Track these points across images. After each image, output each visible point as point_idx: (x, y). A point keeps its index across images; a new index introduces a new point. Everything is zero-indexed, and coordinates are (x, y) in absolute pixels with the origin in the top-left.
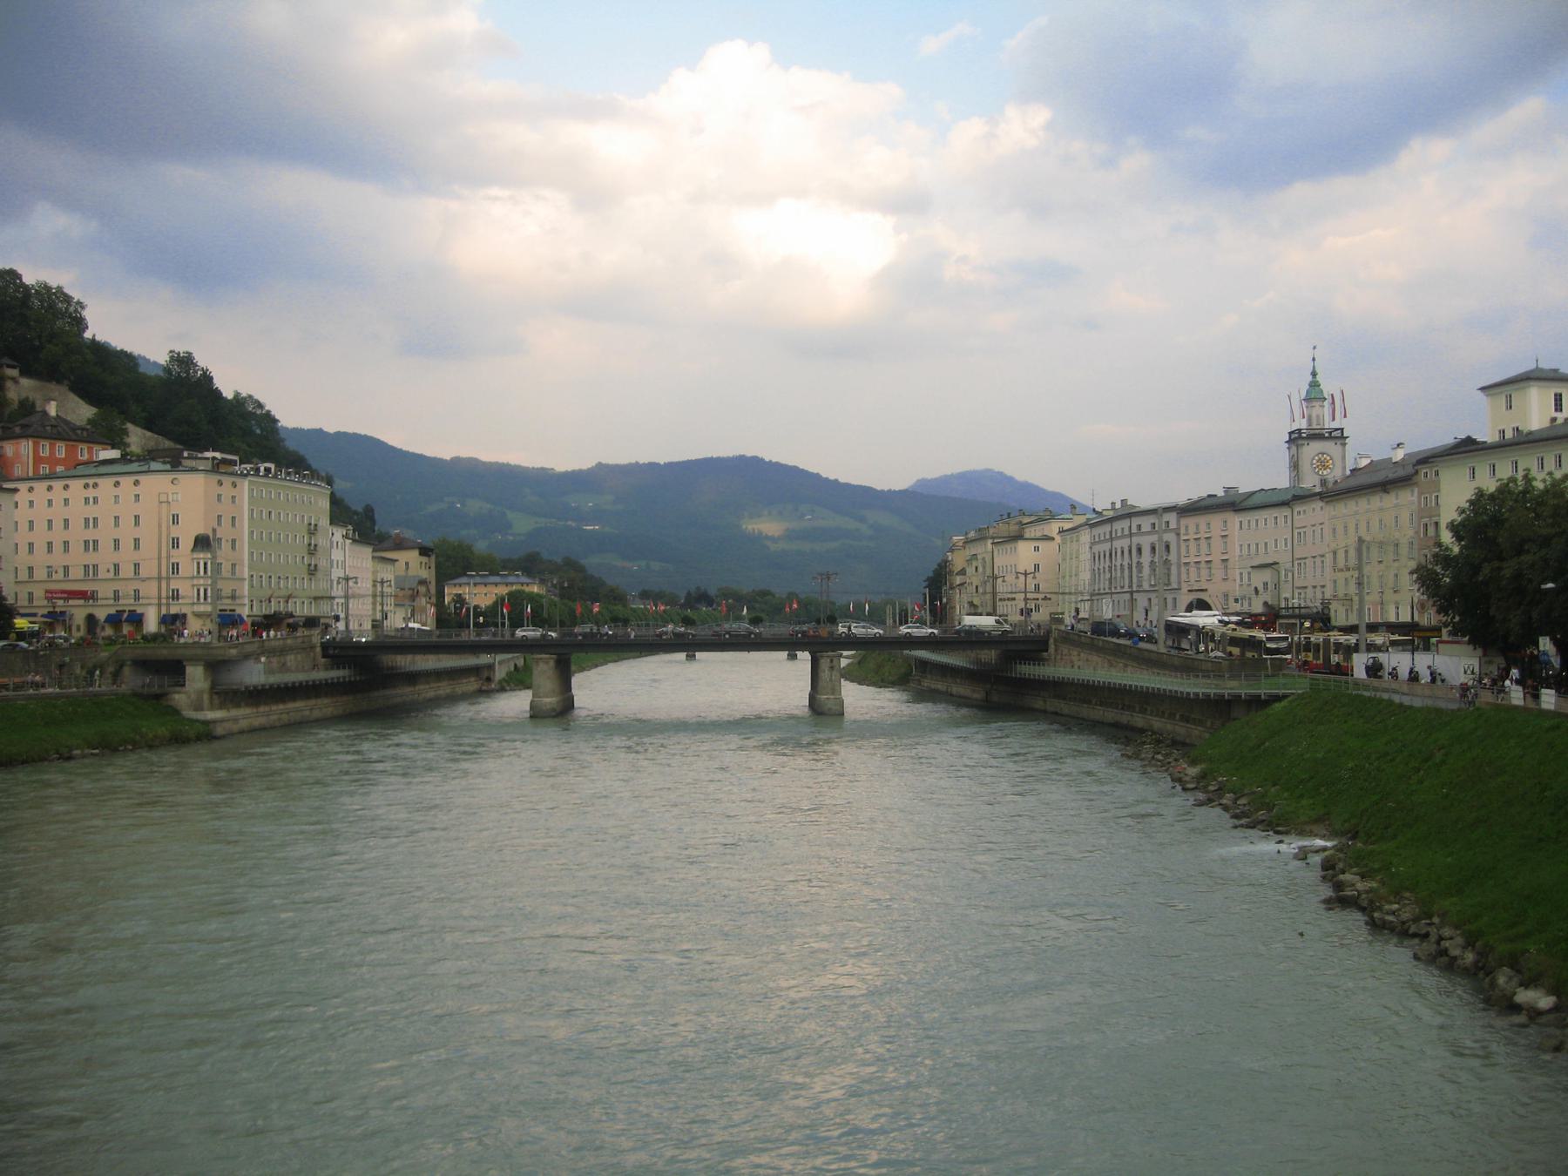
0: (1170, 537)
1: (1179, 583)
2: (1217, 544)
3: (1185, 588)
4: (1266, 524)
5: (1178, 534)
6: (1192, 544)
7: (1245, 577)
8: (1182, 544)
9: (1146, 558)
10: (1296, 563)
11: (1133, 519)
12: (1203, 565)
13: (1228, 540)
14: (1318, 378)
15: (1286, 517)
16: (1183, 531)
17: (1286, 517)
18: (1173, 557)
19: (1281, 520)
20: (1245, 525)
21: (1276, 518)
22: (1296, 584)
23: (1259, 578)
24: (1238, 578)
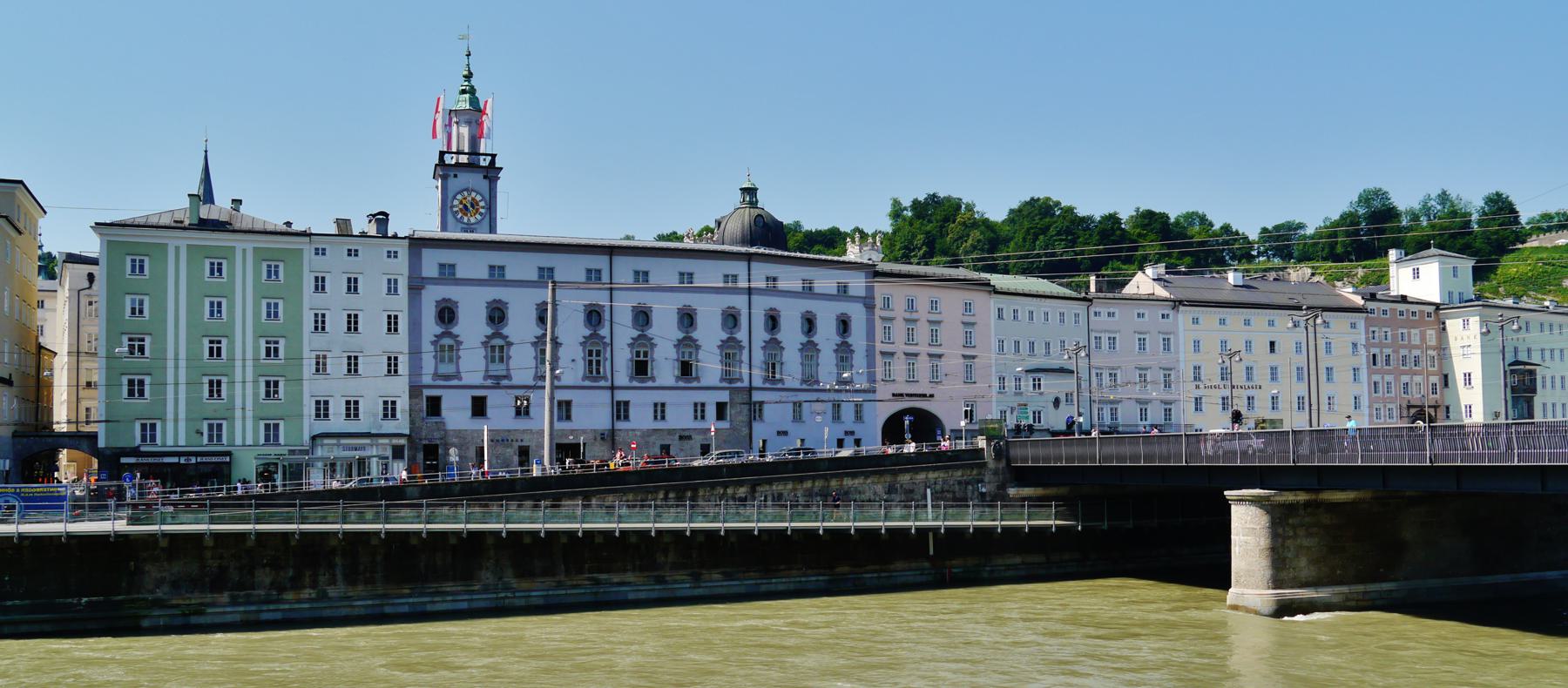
0: (857, 313)
1: (872, 378)
2: (951, 337)
3: (884, 391)
4: (1062, 321)
5: (870, 306)
6: (899, 330)
7: (1010, 384)
8: (878, 323)
9: (791, 334)
10: (1094, 372)
11: (754, 265)
12: (923, 358)
13: (975, 331)
14: (474, 81)
15: (1077, 315)
16: (879, 302)
17: (1077, 315)
18: (857, 338)
19: (1069, 319)
20: (1008, 314)
21: (1062, 314)
22: (1096, 396)
23: (1053, 386)
24: (995, 383)
